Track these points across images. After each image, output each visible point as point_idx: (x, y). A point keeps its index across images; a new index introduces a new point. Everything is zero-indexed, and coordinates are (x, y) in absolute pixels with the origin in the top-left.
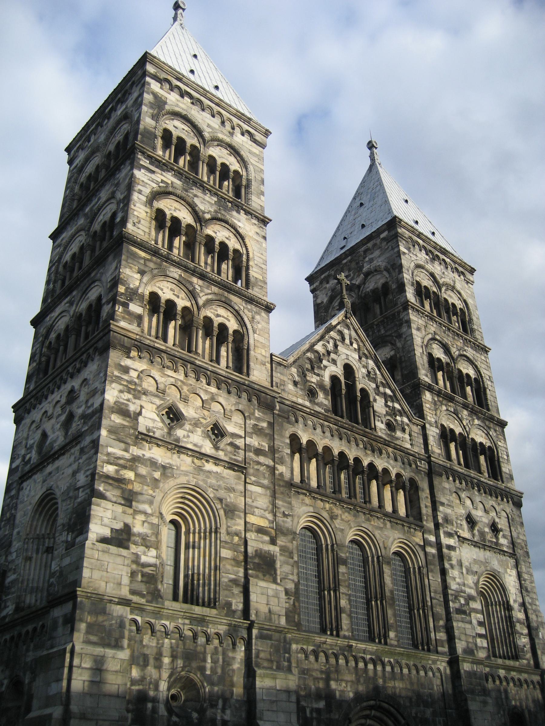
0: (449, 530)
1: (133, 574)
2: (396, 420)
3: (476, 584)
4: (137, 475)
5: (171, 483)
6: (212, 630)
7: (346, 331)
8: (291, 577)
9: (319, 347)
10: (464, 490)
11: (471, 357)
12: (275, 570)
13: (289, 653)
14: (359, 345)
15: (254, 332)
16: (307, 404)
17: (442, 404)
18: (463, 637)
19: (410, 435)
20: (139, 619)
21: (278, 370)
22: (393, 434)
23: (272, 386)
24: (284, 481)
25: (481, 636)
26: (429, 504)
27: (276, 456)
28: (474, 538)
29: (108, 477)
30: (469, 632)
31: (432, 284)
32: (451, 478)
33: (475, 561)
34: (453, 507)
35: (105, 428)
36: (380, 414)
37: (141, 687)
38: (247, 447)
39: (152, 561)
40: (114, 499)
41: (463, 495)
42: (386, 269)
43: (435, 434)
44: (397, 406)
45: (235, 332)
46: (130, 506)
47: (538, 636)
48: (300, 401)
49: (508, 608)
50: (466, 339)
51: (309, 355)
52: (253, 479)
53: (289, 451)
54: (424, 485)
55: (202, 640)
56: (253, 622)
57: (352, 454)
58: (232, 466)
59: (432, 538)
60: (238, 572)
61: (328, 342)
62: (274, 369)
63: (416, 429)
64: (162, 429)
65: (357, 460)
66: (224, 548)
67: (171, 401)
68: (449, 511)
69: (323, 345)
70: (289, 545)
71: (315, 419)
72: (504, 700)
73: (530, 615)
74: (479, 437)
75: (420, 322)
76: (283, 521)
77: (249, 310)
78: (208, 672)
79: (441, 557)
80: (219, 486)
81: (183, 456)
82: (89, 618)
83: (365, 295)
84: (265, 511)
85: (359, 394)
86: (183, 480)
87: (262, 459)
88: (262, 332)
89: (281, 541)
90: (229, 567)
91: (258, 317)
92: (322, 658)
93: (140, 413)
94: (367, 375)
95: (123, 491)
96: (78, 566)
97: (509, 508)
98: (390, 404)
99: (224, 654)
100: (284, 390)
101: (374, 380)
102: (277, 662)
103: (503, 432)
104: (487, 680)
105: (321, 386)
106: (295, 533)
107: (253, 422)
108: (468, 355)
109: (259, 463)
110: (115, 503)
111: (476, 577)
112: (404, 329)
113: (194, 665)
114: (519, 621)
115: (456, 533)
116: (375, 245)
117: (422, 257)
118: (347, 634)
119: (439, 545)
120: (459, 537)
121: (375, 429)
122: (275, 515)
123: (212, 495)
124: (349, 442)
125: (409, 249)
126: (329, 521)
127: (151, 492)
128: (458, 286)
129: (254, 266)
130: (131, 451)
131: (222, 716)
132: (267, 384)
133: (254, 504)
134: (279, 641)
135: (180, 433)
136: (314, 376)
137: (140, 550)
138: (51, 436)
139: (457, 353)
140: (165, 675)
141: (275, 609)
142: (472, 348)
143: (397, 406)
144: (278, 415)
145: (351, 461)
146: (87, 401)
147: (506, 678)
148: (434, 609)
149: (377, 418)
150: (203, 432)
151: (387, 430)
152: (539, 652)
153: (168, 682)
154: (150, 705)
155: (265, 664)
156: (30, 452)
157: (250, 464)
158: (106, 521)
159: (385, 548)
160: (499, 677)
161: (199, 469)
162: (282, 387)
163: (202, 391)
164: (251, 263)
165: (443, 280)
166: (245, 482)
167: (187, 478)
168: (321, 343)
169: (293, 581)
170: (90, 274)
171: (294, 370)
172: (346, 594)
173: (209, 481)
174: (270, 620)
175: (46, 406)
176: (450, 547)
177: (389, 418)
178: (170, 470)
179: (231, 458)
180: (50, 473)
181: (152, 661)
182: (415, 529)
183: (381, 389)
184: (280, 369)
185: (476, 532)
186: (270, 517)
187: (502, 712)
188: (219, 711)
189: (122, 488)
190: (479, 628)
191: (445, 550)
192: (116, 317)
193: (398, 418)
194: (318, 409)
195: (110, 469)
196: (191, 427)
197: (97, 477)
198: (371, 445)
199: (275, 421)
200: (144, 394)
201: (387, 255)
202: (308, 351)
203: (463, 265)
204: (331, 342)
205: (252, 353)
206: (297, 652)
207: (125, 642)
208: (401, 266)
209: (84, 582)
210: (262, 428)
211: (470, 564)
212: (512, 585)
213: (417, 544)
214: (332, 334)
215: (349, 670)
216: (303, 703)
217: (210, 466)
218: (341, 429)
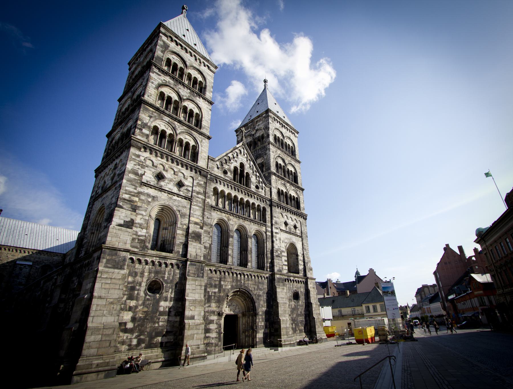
1: (133, 239)
2: (260, 185)
3: (286, 247)
4: (139, 199)
5: (157, 203)
7: (242, 150)
8: (208, 242)
9: (230, 155)
11: (293, 164)
12: (201, 239)
13: (203, 271)
14: (247, 156)
15: (202, 146)
16: (223, 176)
17: (279, 180)
18: (278, 266)
19: (265, 191)
20: (134, 258)
23: (207, 168)
25: (285, 265)
26: (270, 217)
27: (206, 195)
29: (125, 199)
30: (280, 264)
31: (281, 136)
33: (286, 239)
35: (126, 179)
37: (133, 285)
39: (144, 234)
40: (127, 209)
41: (284, 214)
42: (264, 129)
45: (193, 146)
46: (135, 212)
47: (307, 265)
48: (219, 175)
49: (297, 255)
50: (292, 158)
51: (225, 157)
52: (195, 203)
53: (212, 194)
54: (268, 209)
55: (164, 266)
56: (188, 259)
57: (240, 196)
58: (186, 198)
59: (270, 229)
61: (234, 154)
62: (209, 161)
63: (268, 189)
64: (154, 181)
65: (242, 199)
66: (179, 230)
67: (160, 171)
68: (277, 220)
70: (209, 230)
73: (305, 258)
74: (293, 193)
75: (274, 149)
76: (207, 220)
77: (200, 138)
78: (166, 278)
81: (163, 193)
82: (108, 257)
83: (256, 138)
84: (199, 216)
85: (245, 174)
86: (162, 202)
87: (200, 196)
88: (205, 147)
89: (205, 228)
90: (180, 237)
91: (204, 141)
92: (218, 273)
93: (144, 174)
95: (132, 205)
96: (106, 236)
97: (302, 220)
99: (174, 271)
100: (213, 170)
102: (197, 274)
103: (303, 192)
104: (286, 281)
105: (230, 170)
106: (212, 225)
107: (197, 181)
108: (292, 163)
109: (198, 197)
110: (128, 210)
111: (286, 244)
112: (268, 152)
113: (160, 275)
114: (301, 260)
116: (260, 119)
117: (278, 125)
118: (230, 264)
119: (272, 232)
120: (280, 229)
122: (203, 218)
123: (175, 209)
124: (239, 192)
125: (273, 122)
126: (227, 221)
127: (146, 206)
128: (291, 138)
129: (204, 120)
130: (137, 190)
131: (170, 296)
132: (206, 168)
133: (194, 213)
134: (199, 266)
135: (162, 183)
137: (138, 230)
138: (107, 183)
139: (288, 162)
140: (145, 280)
141: (199, 254)
142: (294, 161)
143: (261, 180)
144: (209, 180)
145: (239, 199)
146: (120, 168)
147: (293, 280)
148: (268, 255)
149: (252, 184)
150: (173, 184)
152: (307, 271)
153: (146, 283)
154: (136, 292)
155: (192, 275)
156: (99, 190)
158: (122, 217)
160: (290, 280)
161: (171, 198)
162: (212, 169)
163: (175, 168)
164: (203, 119)
165: (286, 135)
166: (191, 204)
167: (164, 202)
168: (231, 153)
169: (209, 243)
170: (129, 116)
171: (218, 163)
172: (231, 249)
173: (175, 203)
174: (196, 258)
175: (107, 170)
176: (276, 233)
178: (156, 198)
180: (104, 198)
181: (139, 274)
182: (263, 226)
183: (255, 173)
184: (212, 162)
185: (287, 228)
186: (201, 218)
187: (290, 292)
188: (169, 294)
189: (132, 204)
190: (285, 262)
191: (274, 234)
192: (135, 134)
194: (227, 178)
195: (126, 196)
196: (168, 182)
197: (119, 199)
199: (207, 182)
200: (147, 167)
201: (264, 123)
202: (225, 156)
203: (295, 130)
204: (236, 154)
205: (200, 155)
206: (208, 270)
207: (126, 267)
208: (269, 128)
209: (107, 242)
210: (201, 184)
213: (263, 231)
214: (236, 150)
215: (230, 277)
216: (208, 290)
217: (175, 198)
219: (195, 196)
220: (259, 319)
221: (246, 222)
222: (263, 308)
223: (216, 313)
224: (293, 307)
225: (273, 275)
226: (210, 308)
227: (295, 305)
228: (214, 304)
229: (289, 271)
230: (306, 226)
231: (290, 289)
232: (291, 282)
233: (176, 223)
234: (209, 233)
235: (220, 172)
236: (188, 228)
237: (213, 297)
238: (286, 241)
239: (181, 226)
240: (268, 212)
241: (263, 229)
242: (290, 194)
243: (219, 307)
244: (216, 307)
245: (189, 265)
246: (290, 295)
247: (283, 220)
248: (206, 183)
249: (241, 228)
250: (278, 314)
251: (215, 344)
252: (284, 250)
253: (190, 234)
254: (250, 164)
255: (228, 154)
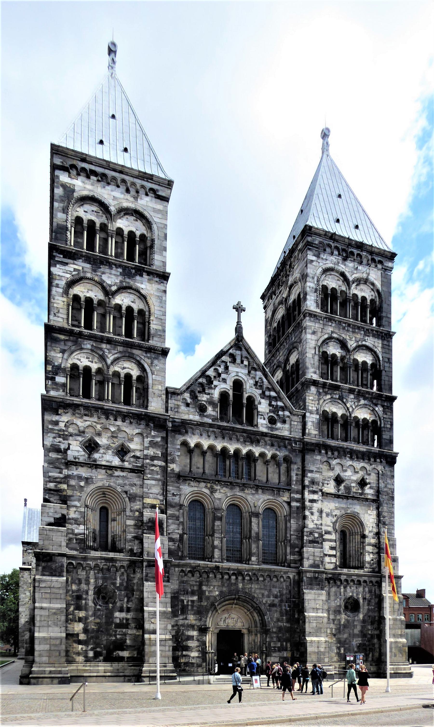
0: (314, 489)
2: (278, 415)
3: (334, 523)
6: (119, 564)
8: (177, 531)
9: (211, 373)
10: (335, 459)
14: (249, 362)
21: (173, 398)
22: (274, 426)
23: (167, 411)
24: (174, 474)
26: (300, 473)
27: (169, 458)
28: (338, 492)
32: (323, 452)
33: (337, 509)
34: (321, 472)
36: (263, 413)
38: (146, 457)
43: (314, 420)
44: (280, 404)
48: (191, 417)
49: (364, 536)
51: (200, 380)
52: (149, 476)
57: (232, 448)
60: (138, 532)
66: (128, 519)
69: (215, 369)
70: (177, 513)
71: (201, 428)
72: (342, 594)
76: (173, 499)
79: (303, 508)
80: (125, 484)
85: (245, 401)
87: (156, 462)
94: (255, 385)
98: (274, 403)
99: (128, 576)
101: (261, 387)
105: (211, 402)
111: (335, 518)
115: (321, 490)
119: (303, 500)
121: (257, 425)
122: (166, 497)
133: (150, 491)
136: (205, 395)
143: (280, 404)
145: (232, 452)
149: (260, 417)
151: (268, 424)
155: (152, 580)
157: (147, 467)
159: (255, 507)
160: (341, 580)
162: (176, 410)
168: (212, 369)
171: (187, 396)
177: (272, 414)
179: (134, 465)
183: (267, 393)
185: (342, 487)
186: (161, 498)
191: (307, 503)
193: (281, 413)
198: (250, 438)
199: (169, 434)
202: (200, 377)
211: (331, 510)
212: (371, 521)
213: (284, 501)
214: (224, 358)
218: (224, 431)
219: (147, 464)
220: (272, 638)
221: (246, 491)
222: (279, 623)
223: (196, 627)
224: (342, 623)
225: (300, 573)
226: (186, 622)
227: (348, 621)
228: (192, 616)
229: (344, 564)
230: (393, 476)
231: (338, 594)
232: (341, 583)
233: (124, 510)
234: (177, 518)
235: (192, 410)
236: (141, 514)
237: (190, 608)
238: (337, 512)
239: (131, 514)
240: (295, 463)
241: (285, 497)
242: (356, 418)
243: (200, 620)
244: (195, 620)
245: (146, 567)
246: (338, 604)
247: (332, 474)
248: (165, 439)
249: (240, 502)
250: (305, 632)
251: (197, 664)
252: (330, 529)
253: (145, 523)
254: (254, 378)
255: (206, 371)
